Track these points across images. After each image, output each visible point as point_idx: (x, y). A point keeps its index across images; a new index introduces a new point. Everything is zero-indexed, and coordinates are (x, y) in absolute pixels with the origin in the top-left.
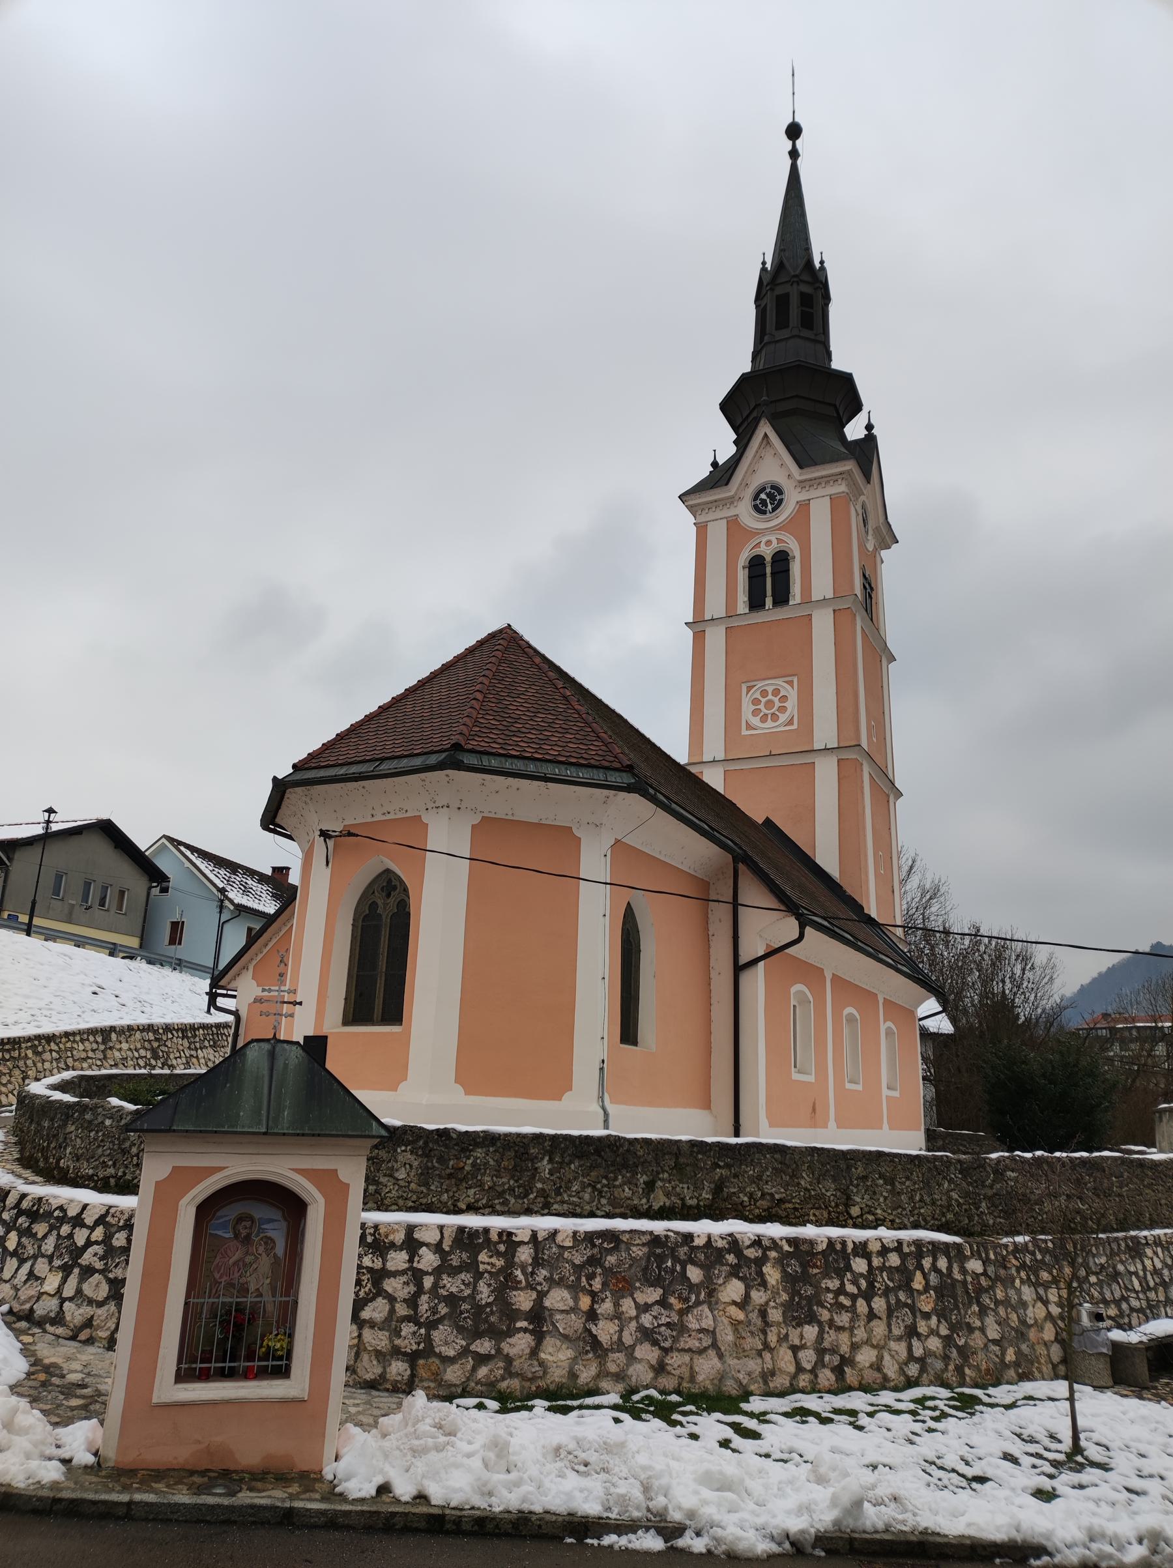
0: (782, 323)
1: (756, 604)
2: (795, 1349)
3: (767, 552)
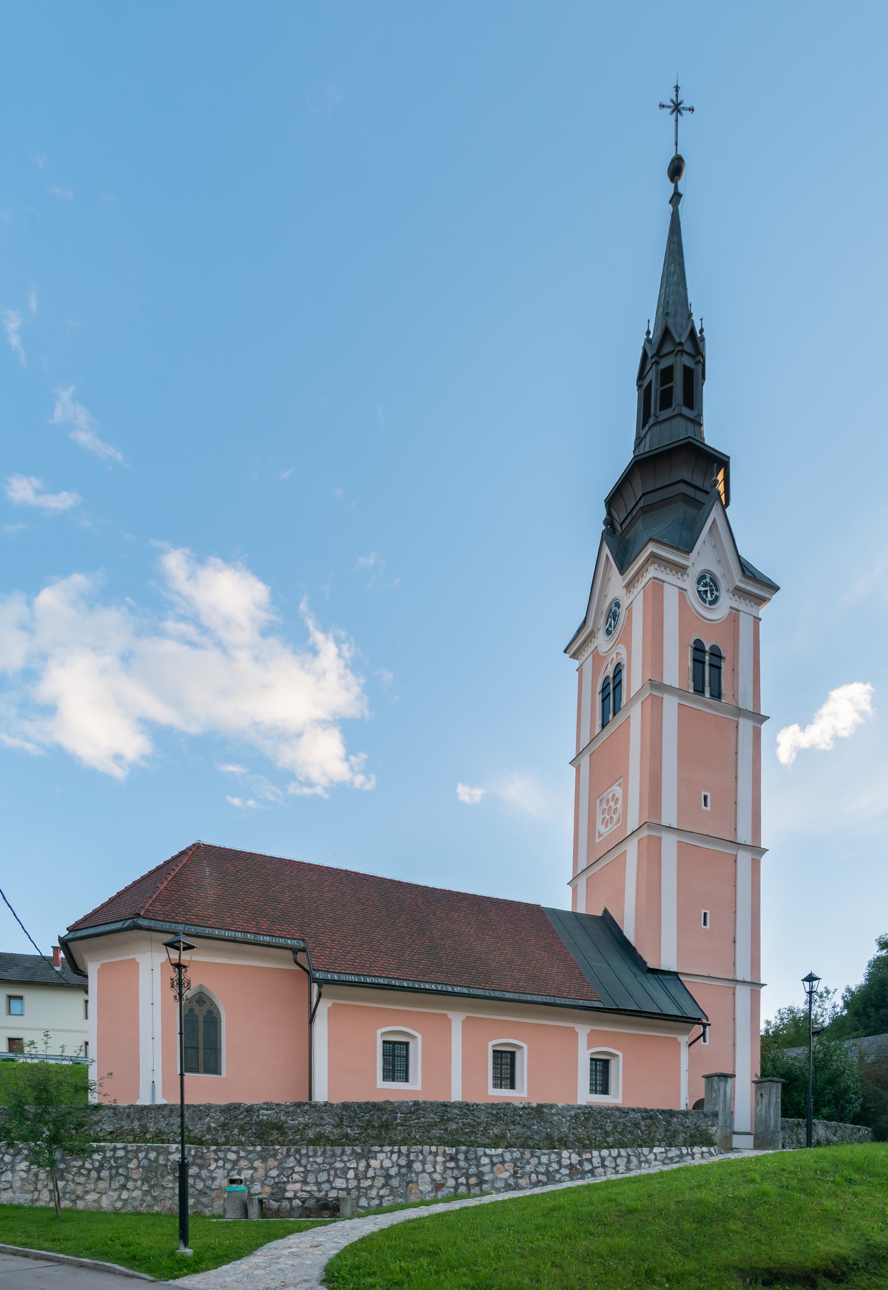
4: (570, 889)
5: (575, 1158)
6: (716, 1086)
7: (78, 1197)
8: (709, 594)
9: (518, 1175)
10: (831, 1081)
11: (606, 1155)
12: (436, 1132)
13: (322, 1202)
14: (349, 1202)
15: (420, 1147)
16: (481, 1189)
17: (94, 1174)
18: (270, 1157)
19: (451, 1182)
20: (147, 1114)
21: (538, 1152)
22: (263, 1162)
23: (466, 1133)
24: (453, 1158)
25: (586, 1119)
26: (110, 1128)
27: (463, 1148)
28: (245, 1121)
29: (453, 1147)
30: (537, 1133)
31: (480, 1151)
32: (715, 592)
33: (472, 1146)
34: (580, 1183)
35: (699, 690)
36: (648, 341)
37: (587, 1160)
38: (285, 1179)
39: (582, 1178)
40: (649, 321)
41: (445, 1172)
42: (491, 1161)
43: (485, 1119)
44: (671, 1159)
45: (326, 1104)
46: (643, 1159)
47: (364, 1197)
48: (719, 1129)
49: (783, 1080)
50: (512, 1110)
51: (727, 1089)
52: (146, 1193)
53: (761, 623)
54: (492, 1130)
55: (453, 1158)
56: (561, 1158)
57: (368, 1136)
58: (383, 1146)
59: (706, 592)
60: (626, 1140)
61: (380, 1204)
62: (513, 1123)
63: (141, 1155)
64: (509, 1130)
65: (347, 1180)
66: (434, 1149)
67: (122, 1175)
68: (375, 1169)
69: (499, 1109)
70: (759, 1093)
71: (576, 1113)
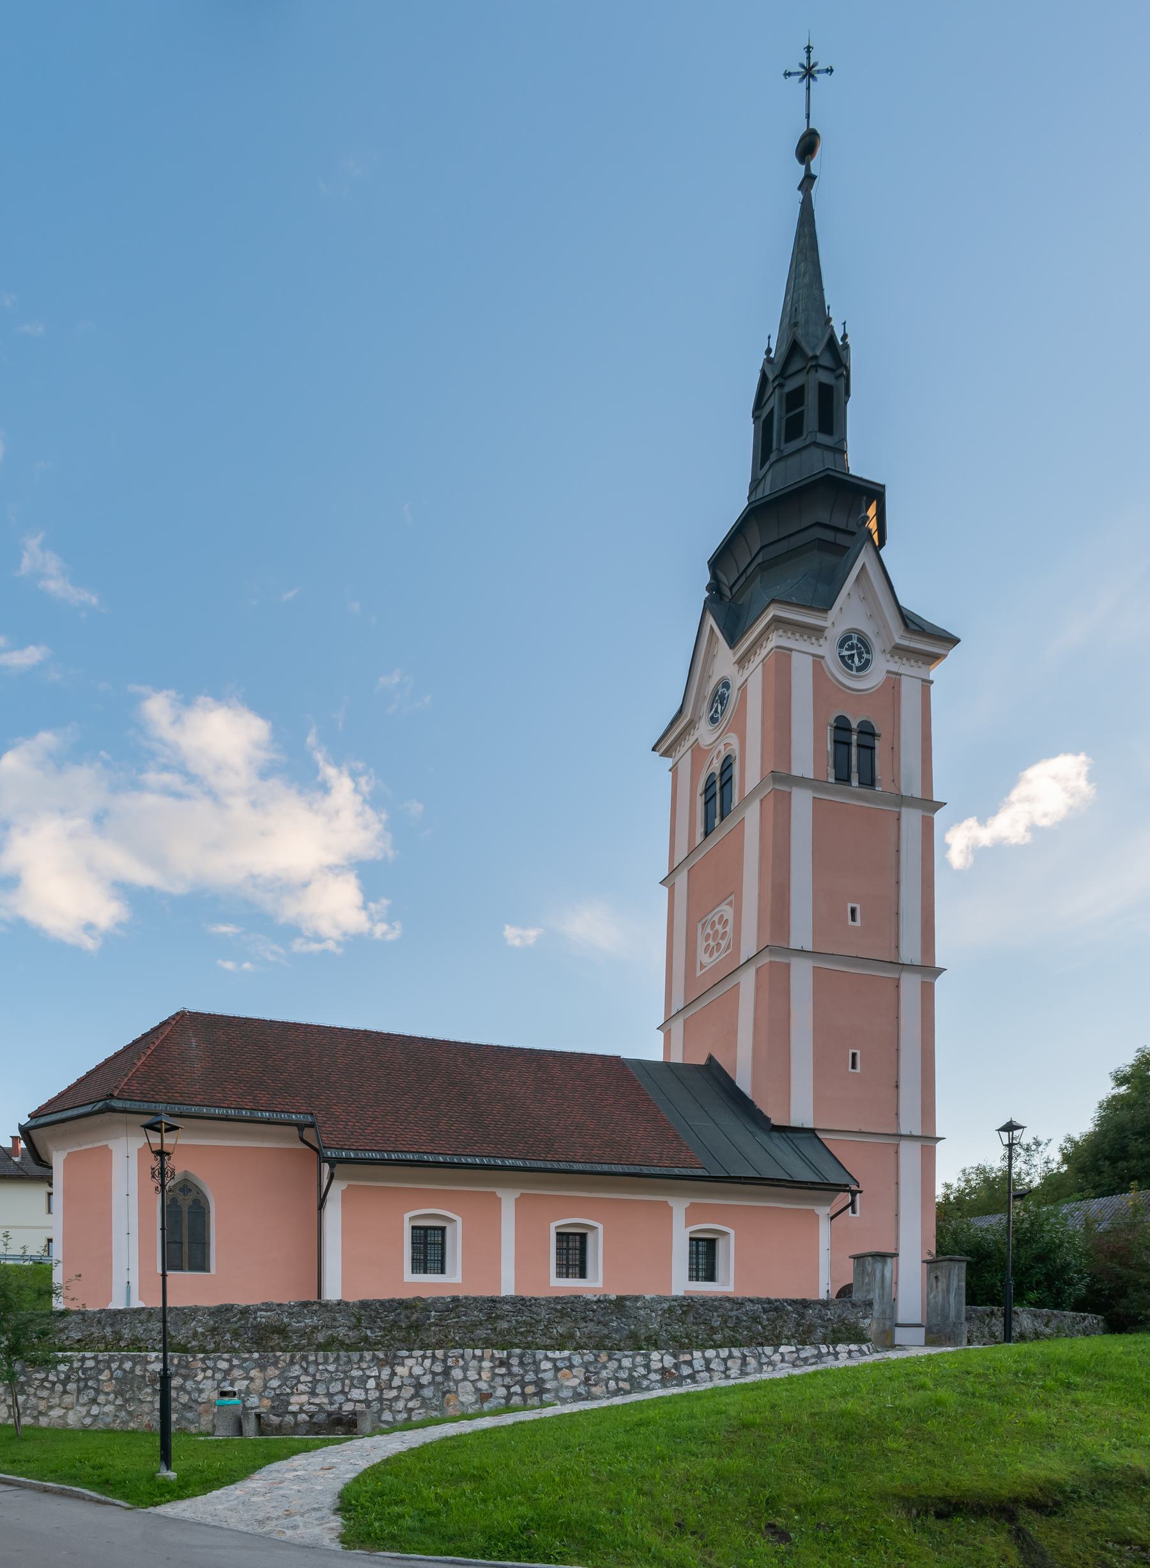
4: (661, 1034)
5: (669, 1361)
6: (869, 1269)
7: (41, 1413)
8: (856, 659)
9: (590, 1382)
10: (1041, 1258)
11: (712, 1357)
12: (481, 1333)
13: (335, 1416)
14: (368, 1417)
15: (461, 1351)
16: (541, 1400)
17: (59, 1388)
18: (270, 1365)
19: (501, 1392)
20: (121, 1319)
21: (618, 1354)
22: (261, 1371)
23: (522, 1333)
24: (503, 1363)
25: (684, 1312)
26: (77, 1335)
27: (518, 1351)
28: (239, 1324)
29: (503, 1349)
30: (617, 1331)
31: (540, 1354)
32: (865, 656)
33: (529, 1348)
34: (675, 1390)
35: (843, 777)
36: (769, 361)
37: (685, 1362)
38: (288, 1390)
39: (679, 1385)
40: (769, 337)
41: (493, 1379)
42: (555, 1366)
43: (547, 1316)
44: (805, 1360)
45: (339, 1303)
46: (764, 1360)
47: (387, 1411)
48: (875, 1322)
49: (969, 1258)
50: (583, 1303)
51: (885, 1272)
52: (120, 1408)
53: (932, 687)
54: (556, 1328)
55: (503, 1363)
56: (650, 1360)
57: (393, 1338)
58: (413, 1350)
59: (853, 655)
60: (741, 1338)
61: (409, 1418)
62: (584, 1319)
63: (114, 1366)
64: (579, 1328)
65: (367, 1390)
66: (478, 1352)
67: (91, 1388)
68: (402, 1377)
69: (565, 1303)
70: (933, 1276)
71: (670, 1306)
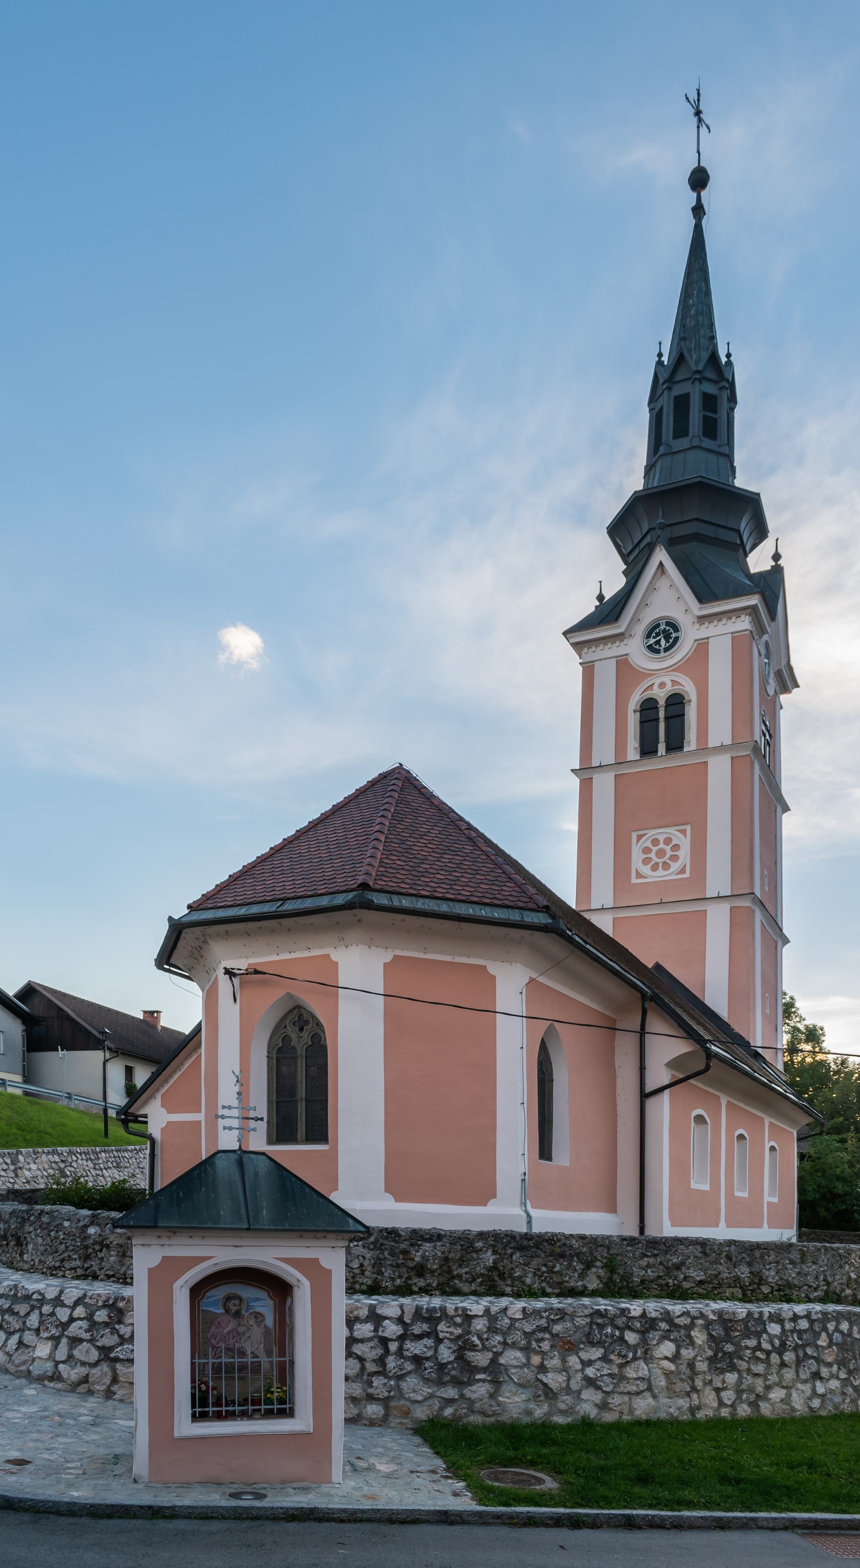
0: (681, 431)
1: (647, 750)
2: (718, 1390)
3: (661, 695)
17: (775, 1358)
